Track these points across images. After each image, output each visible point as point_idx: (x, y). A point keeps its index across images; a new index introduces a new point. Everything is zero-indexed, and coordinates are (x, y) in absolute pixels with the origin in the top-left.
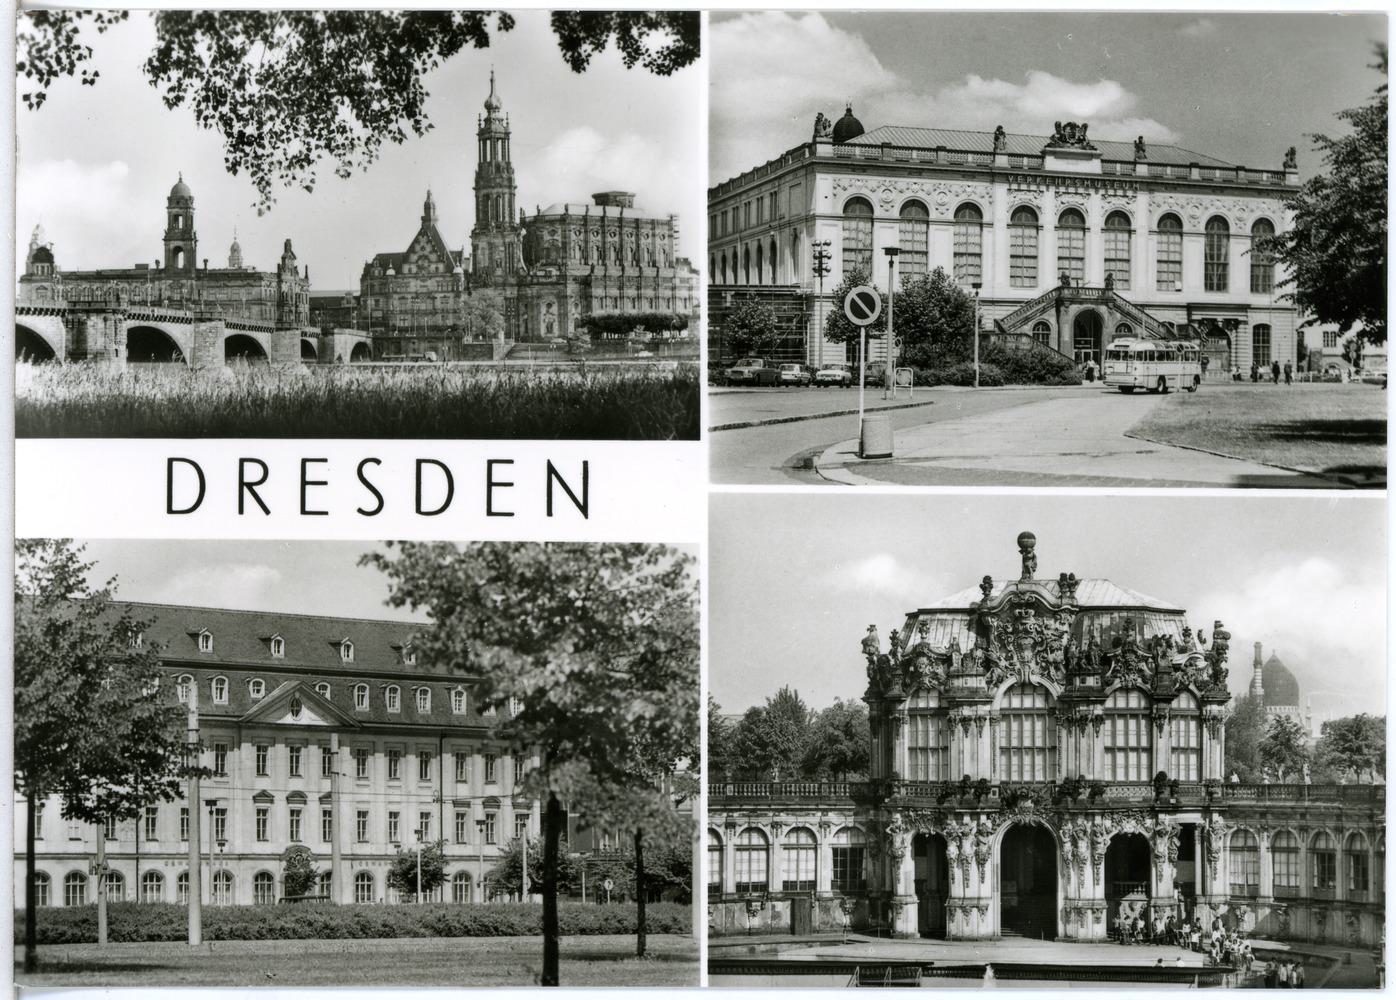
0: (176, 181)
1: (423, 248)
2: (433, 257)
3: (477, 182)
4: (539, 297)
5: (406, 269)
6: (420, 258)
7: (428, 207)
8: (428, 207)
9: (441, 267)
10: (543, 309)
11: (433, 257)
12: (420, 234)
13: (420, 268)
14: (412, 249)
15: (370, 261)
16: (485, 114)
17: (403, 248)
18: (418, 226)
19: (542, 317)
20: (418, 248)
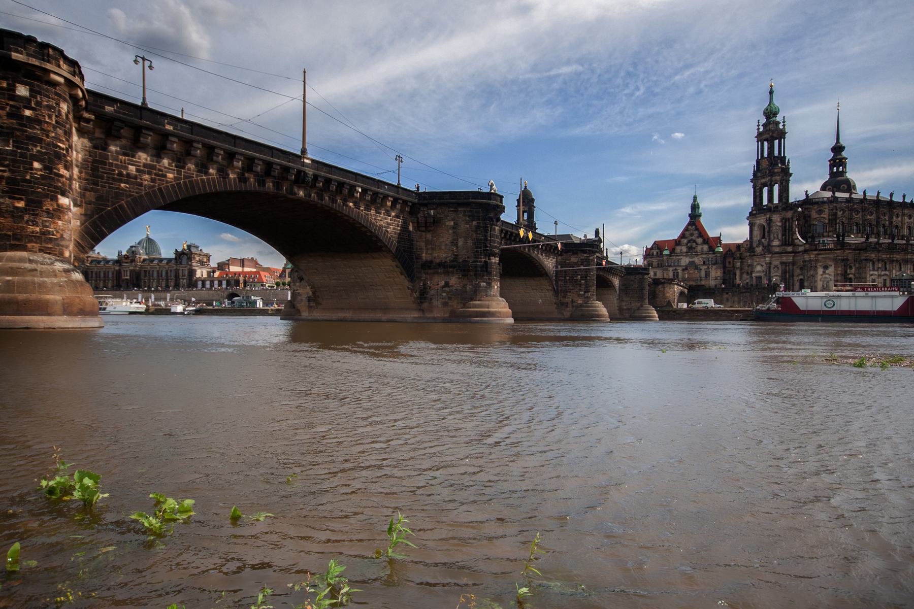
1: (692, 235)
2: (700, 240)
3: (755, 174)
4: (817, 261)
5: (678, 249)
6: (689, 242)
7: (695, 207)
8: (695, 207)
9: (706, 247)
10: (820, 271)
11: (700, 240)
12: (689, 224)
13: (690, 248)
14: (683, 236)
15: (649, 247)
16: (763, 120)
19: (819, 277)
20: (687, 233)
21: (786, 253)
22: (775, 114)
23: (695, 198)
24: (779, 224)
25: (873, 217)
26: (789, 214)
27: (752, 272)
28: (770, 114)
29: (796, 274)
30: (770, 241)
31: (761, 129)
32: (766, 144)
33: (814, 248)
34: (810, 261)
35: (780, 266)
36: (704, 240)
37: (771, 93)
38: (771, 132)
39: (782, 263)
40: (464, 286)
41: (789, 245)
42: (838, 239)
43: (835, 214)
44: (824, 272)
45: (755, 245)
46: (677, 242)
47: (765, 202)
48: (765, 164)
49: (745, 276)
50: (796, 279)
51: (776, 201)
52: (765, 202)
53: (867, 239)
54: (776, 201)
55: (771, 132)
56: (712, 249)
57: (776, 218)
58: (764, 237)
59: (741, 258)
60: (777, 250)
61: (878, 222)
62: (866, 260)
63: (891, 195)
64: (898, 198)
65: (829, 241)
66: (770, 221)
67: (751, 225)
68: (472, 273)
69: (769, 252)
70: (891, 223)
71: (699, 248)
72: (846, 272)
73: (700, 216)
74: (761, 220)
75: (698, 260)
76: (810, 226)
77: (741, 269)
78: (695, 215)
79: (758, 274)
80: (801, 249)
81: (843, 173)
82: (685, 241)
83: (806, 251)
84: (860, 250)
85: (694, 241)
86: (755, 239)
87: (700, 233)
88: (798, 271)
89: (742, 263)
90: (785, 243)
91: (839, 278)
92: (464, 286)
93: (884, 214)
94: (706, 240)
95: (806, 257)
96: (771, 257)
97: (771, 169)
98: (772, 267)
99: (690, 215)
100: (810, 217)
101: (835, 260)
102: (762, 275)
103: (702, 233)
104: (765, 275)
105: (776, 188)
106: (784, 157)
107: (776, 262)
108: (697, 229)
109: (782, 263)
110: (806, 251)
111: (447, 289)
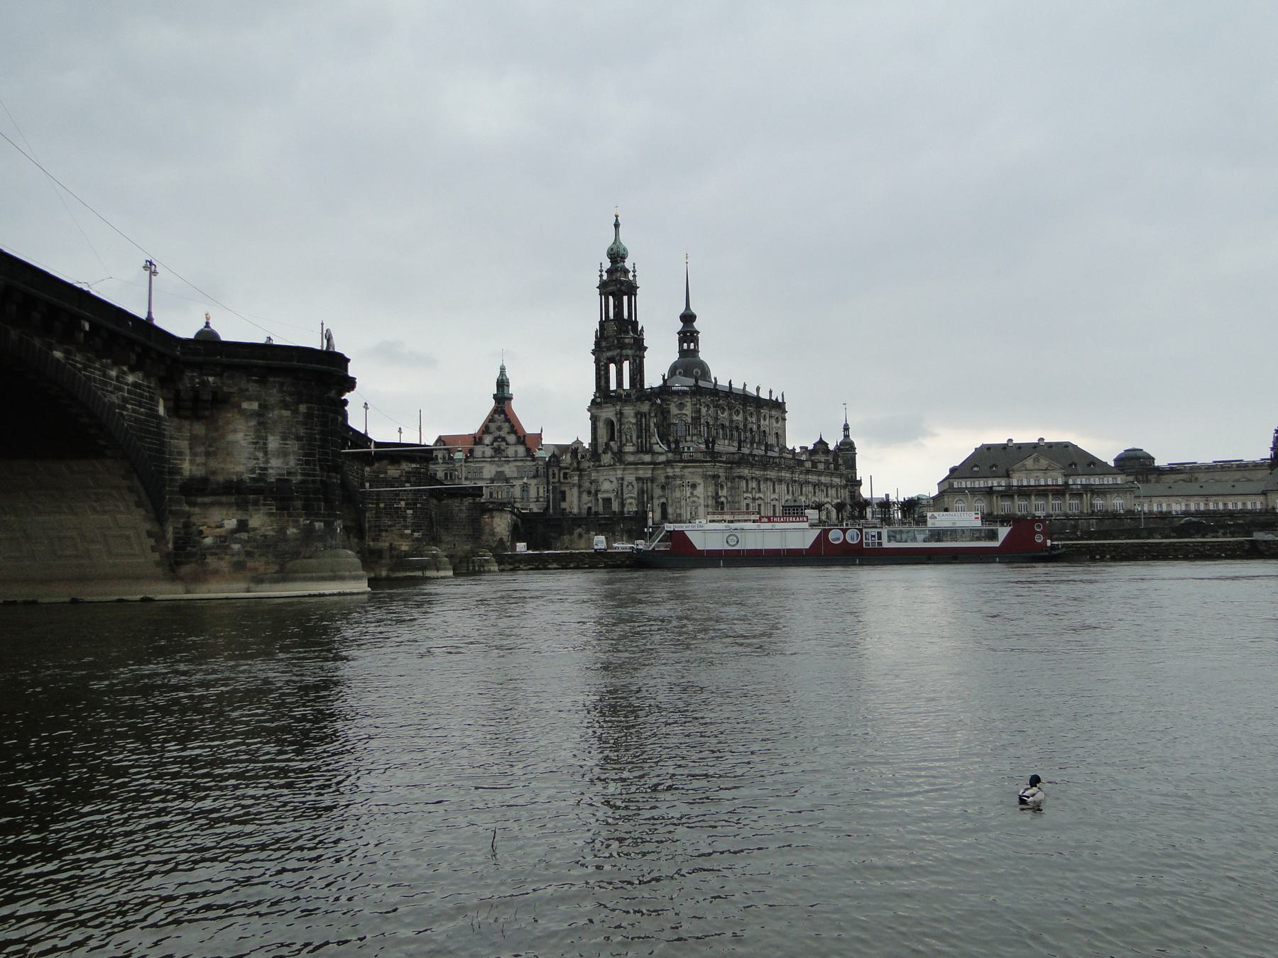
0: (201, 326)
1: (499, 429)
2: (512, 438)
3: (597, 344)
5: (479, 450)
6: (495, 439)
7: (502, 384)
8: (502, 384)
9: (521, 450)
11: (512, 438)
13: (498, 451)
14: (486, 429)
16: (607, 264)
17: (473, 427)
18: (492, 404)
20: (493, 426)
21: (643, 463)
22: (623, 258)
23: (503, 370)
24: (634, 421)
25: (740, 418)
26: (645, 407)
27: (597, 492)
28: (617, 256)
29: (656, 495)
30: (622, 446)
31: (605, 277)
32: (611, 298)
33: (678, 457)
34: (674, 477)
35: (635, 483)
36: (519, 438)
37: (617, 225)
38: (618, 284)
39: (638, 479)
40: (282, 530)
41: (647, 452)
42: (707, 447)
43: (699, 411)
45: (600, 451)
46: (477, 440)
47: (613, 386)
48: (612, 328)
49: (585, 497)
50: (656, 502)
51: (626, 385)
52: (613, 386)
53: (739, 448)
54: (626, 385)
55: (618, 284)
56: (529, 452)
57: (629, 411)
58: (612, 438)
59: (578, 469)
60: (631, 458)
61: (745, 426)
62: (740, 477)
63: (758, 389)
64: (764, 395)
65: (694, 445)
66: (621, 413)
67: (594, 419)
68: (299, 504)
69: (621, 461)
70: (759, 427)
71: (511, 451)
72: (717, 493)
73: (511, 399)
74: (608, 413)
75: (509, 470)
76: (669, 425)
77: (580, 486)
78: (502, 397)
79: (605, 496)
80: (662, 458)
81: (696, 351)
82: (488, 439)
83: (668, 463)
84: (731, 463)
85: (504, 439)
86: (600, 441)
87: (512, 426)
88: (658, 492)
89: (580, 476)
90: (641, 450)
91: (710, 502)
92: (282, 530)
93: (751, 415)
94: (522, 439)
95: (670, 471)
96: (624, 470)
97: (618, 339)
98: (625, 483)
99: (495, 397)
100: (669, 412)
101: (705, 477)
102: (612, 496)
103: (515, 428)
104: (617, 496)
105: (626, 365)
106: (636, 323)
107: (630, 477)
108: (507, 420)
109: (638, 479)
110: (668, 463)
111: (244, 536)
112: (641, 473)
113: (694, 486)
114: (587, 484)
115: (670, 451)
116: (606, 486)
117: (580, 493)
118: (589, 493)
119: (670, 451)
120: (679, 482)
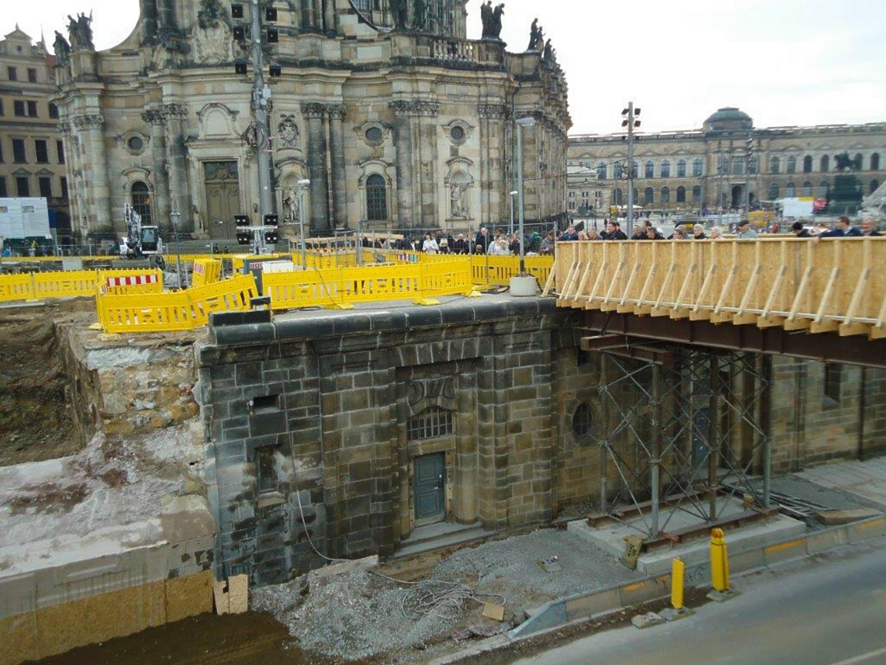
21: (321, 64)
27: (182, 146)
33: (424, 52)
34: (418, 106)
35: (299, 119)
44: (454, 152)
49: (121, 152)
59: (99, 79)
77: (105, 126)
88: (358, 145)
89: (104, 96)
95: (402, 87)
101: (484, 109)
102: (239, 153)
107: (288, 105)
110: (400, 64)
112: (315, 92)
113: (458, 133)
114: (127, 119)
115: (400, 28)
116: (216, 124)
117: (108, 144)
118: (134, 144)
119: (400, 28)
120: (426, 121)
